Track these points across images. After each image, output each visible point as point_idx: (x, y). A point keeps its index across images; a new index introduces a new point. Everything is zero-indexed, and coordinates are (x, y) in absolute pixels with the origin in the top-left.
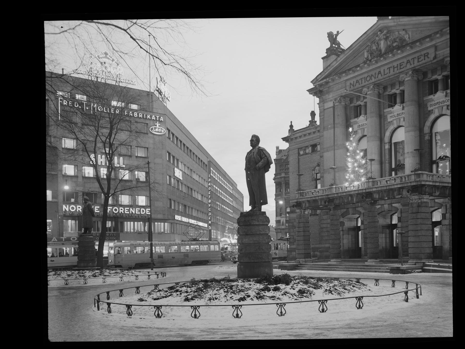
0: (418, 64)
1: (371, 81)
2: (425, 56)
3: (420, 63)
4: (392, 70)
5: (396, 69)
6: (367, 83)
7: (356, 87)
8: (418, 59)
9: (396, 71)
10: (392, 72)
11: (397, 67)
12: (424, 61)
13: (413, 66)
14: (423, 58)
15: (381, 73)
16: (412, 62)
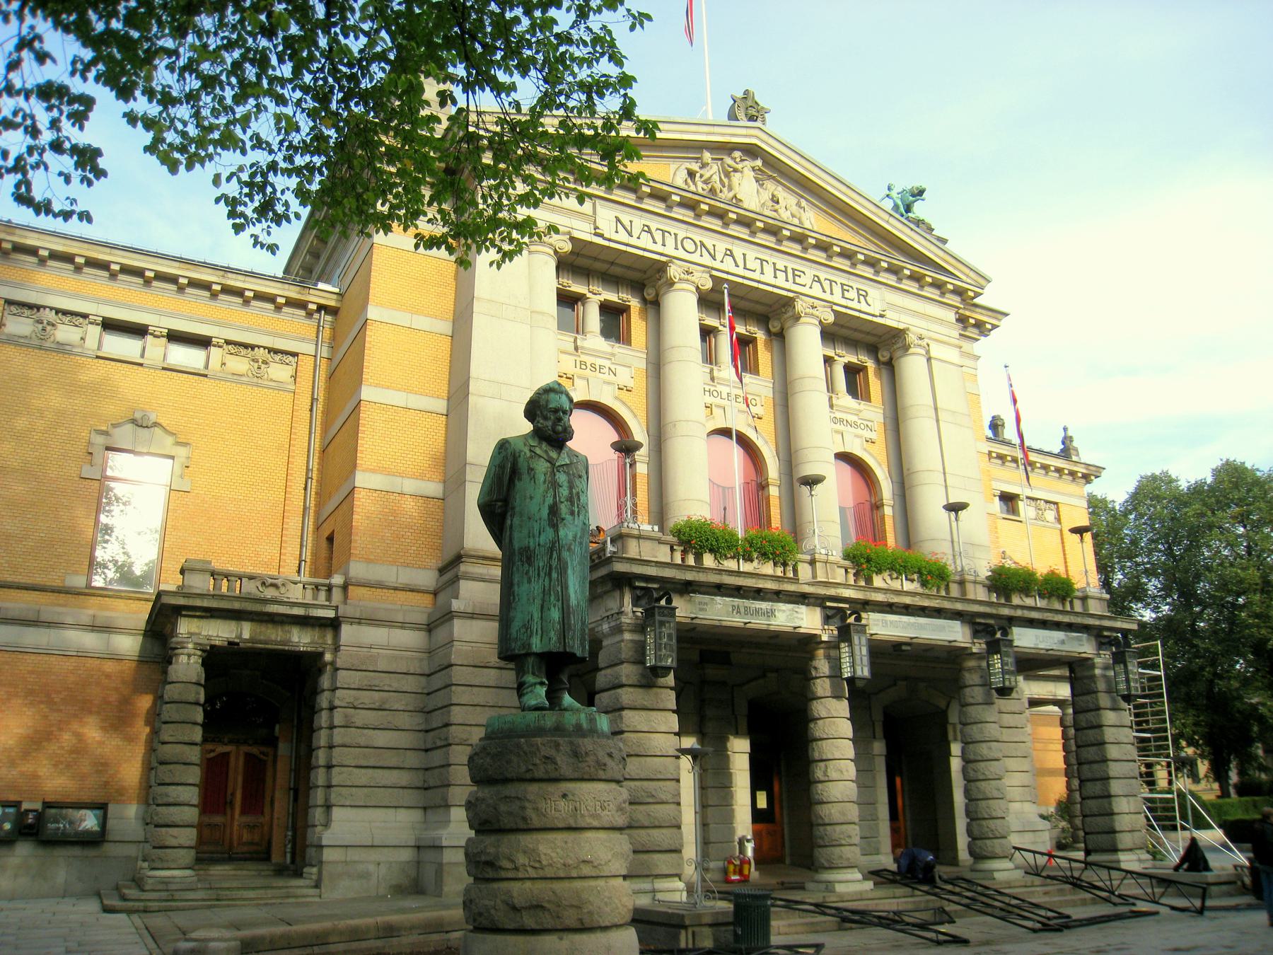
0: (844, 302)
1: (695, 258)
2: (859, 295)
3: (850, 304)
4: (768, 269)
5: (781, 275)
6: (681, 253)
7: (633, 241)
8: (843, 290)
9: (780, 281)
10: (768, 277)
11: (786, 272)
12: (854, 305)
13: (827, 297)
14: (852, 294)
15: (732, 255)
16: (826, 285)
